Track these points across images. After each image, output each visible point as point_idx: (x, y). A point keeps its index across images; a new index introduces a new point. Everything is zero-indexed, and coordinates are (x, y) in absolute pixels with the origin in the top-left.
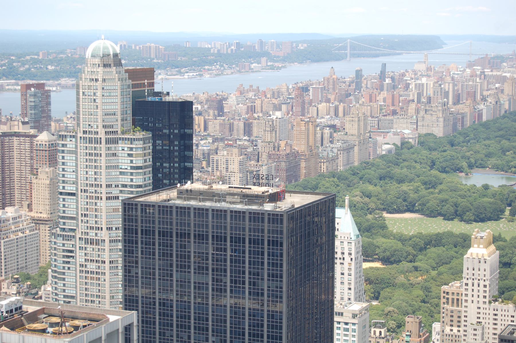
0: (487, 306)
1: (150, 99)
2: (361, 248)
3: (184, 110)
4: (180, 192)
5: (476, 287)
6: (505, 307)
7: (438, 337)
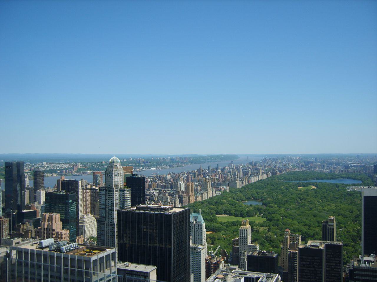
2: (205, 227)
3: (142, 180)
4: (137, 208)
7: (231, 257)
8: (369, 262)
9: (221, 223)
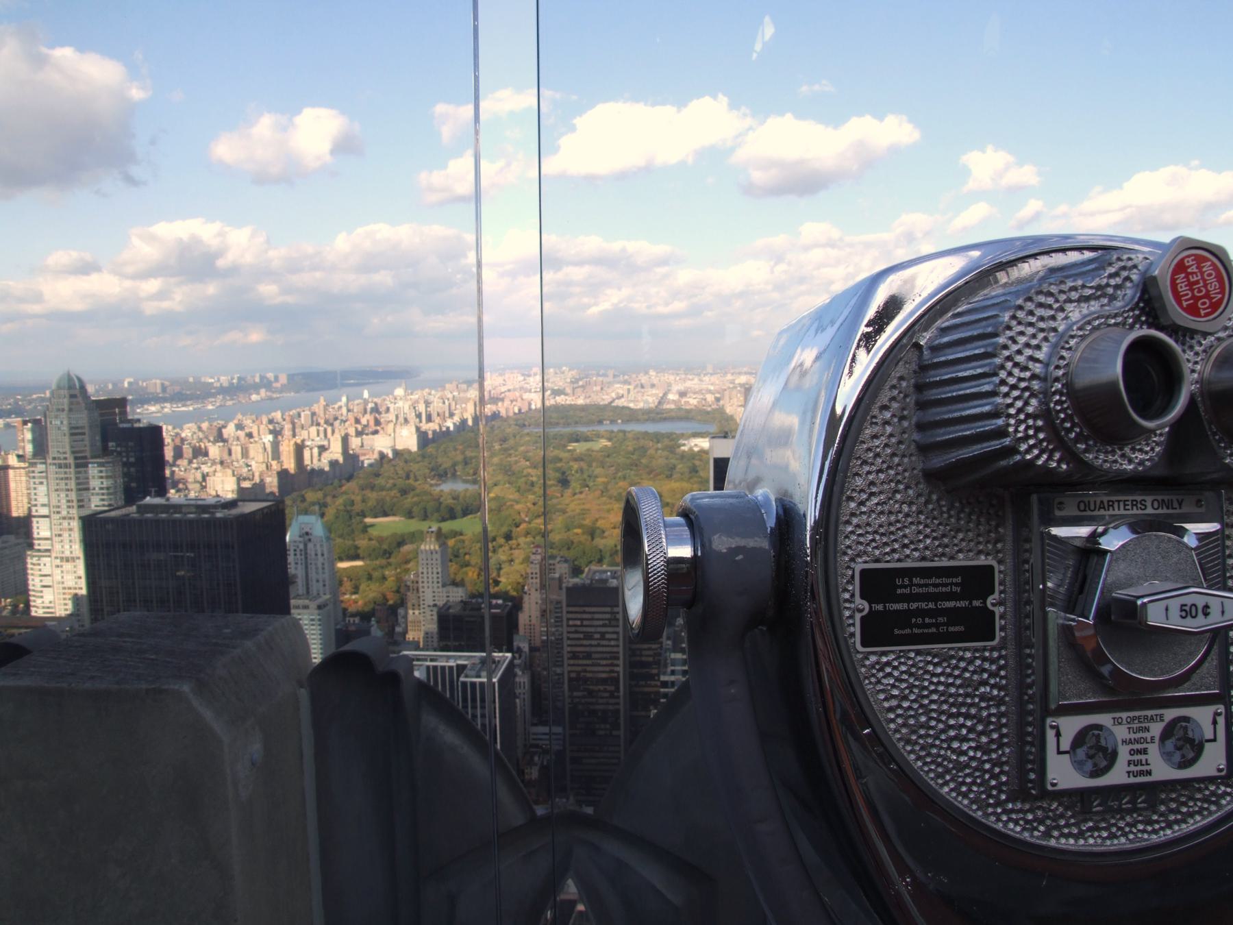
1: (122, 425)
4: (139, 507)
9: (381, 540)
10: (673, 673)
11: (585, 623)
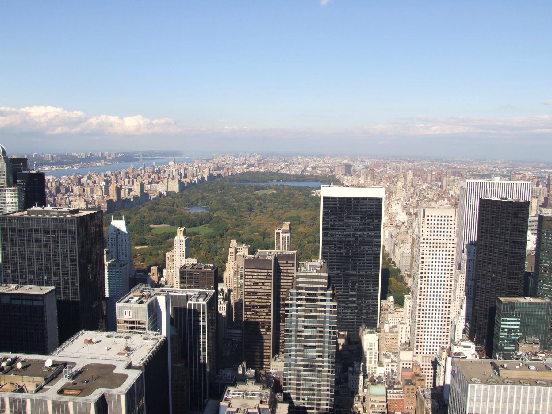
0: (185, 259)
1: (24, 172)
4: (29, 211)
5: (179, 252)
6: (192, 260)
8: (314, 267)
9: (157, 236)
10: (291, 299)
11: (254, 277)
